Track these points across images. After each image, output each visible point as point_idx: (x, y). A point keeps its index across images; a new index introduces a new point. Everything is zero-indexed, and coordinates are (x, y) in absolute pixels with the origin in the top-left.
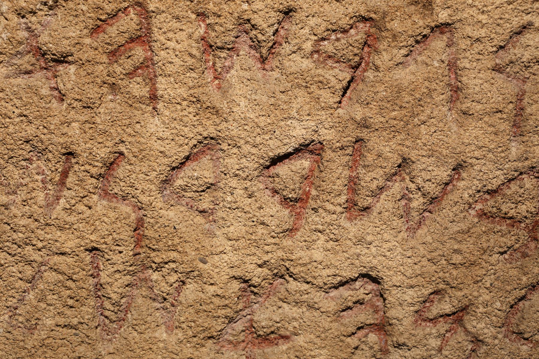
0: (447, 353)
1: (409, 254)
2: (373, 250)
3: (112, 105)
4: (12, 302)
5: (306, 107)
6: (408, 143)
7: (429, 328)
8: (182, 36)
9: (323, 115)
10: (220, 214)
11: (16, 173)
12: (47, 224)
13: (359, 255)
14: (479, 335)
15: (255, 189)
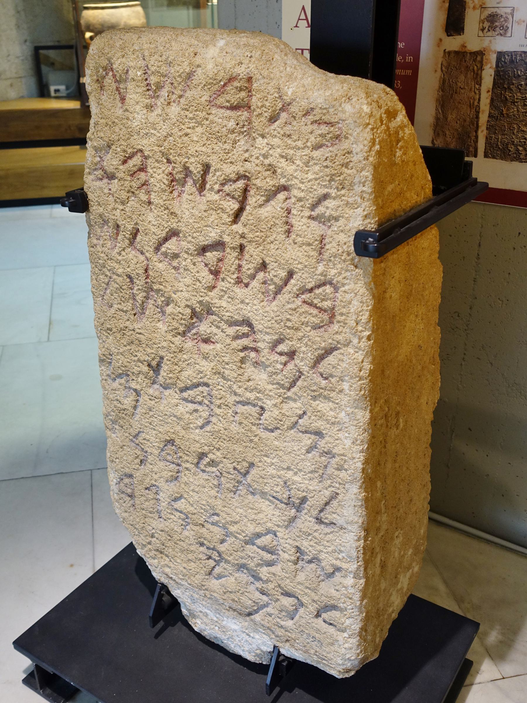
0: (285, 373)
1: (266, 315)
2: (249, 308)
3: (133, 203)
4: (102, 293)
5: (216, 221)
6: (265, 252)
7: (277, 357)
8: (160, 171)
9: (224, 228)
11: (99, 230)
12: (111, 259)
13: (242, 309)
14: (301, 369)
15: (196, 260)
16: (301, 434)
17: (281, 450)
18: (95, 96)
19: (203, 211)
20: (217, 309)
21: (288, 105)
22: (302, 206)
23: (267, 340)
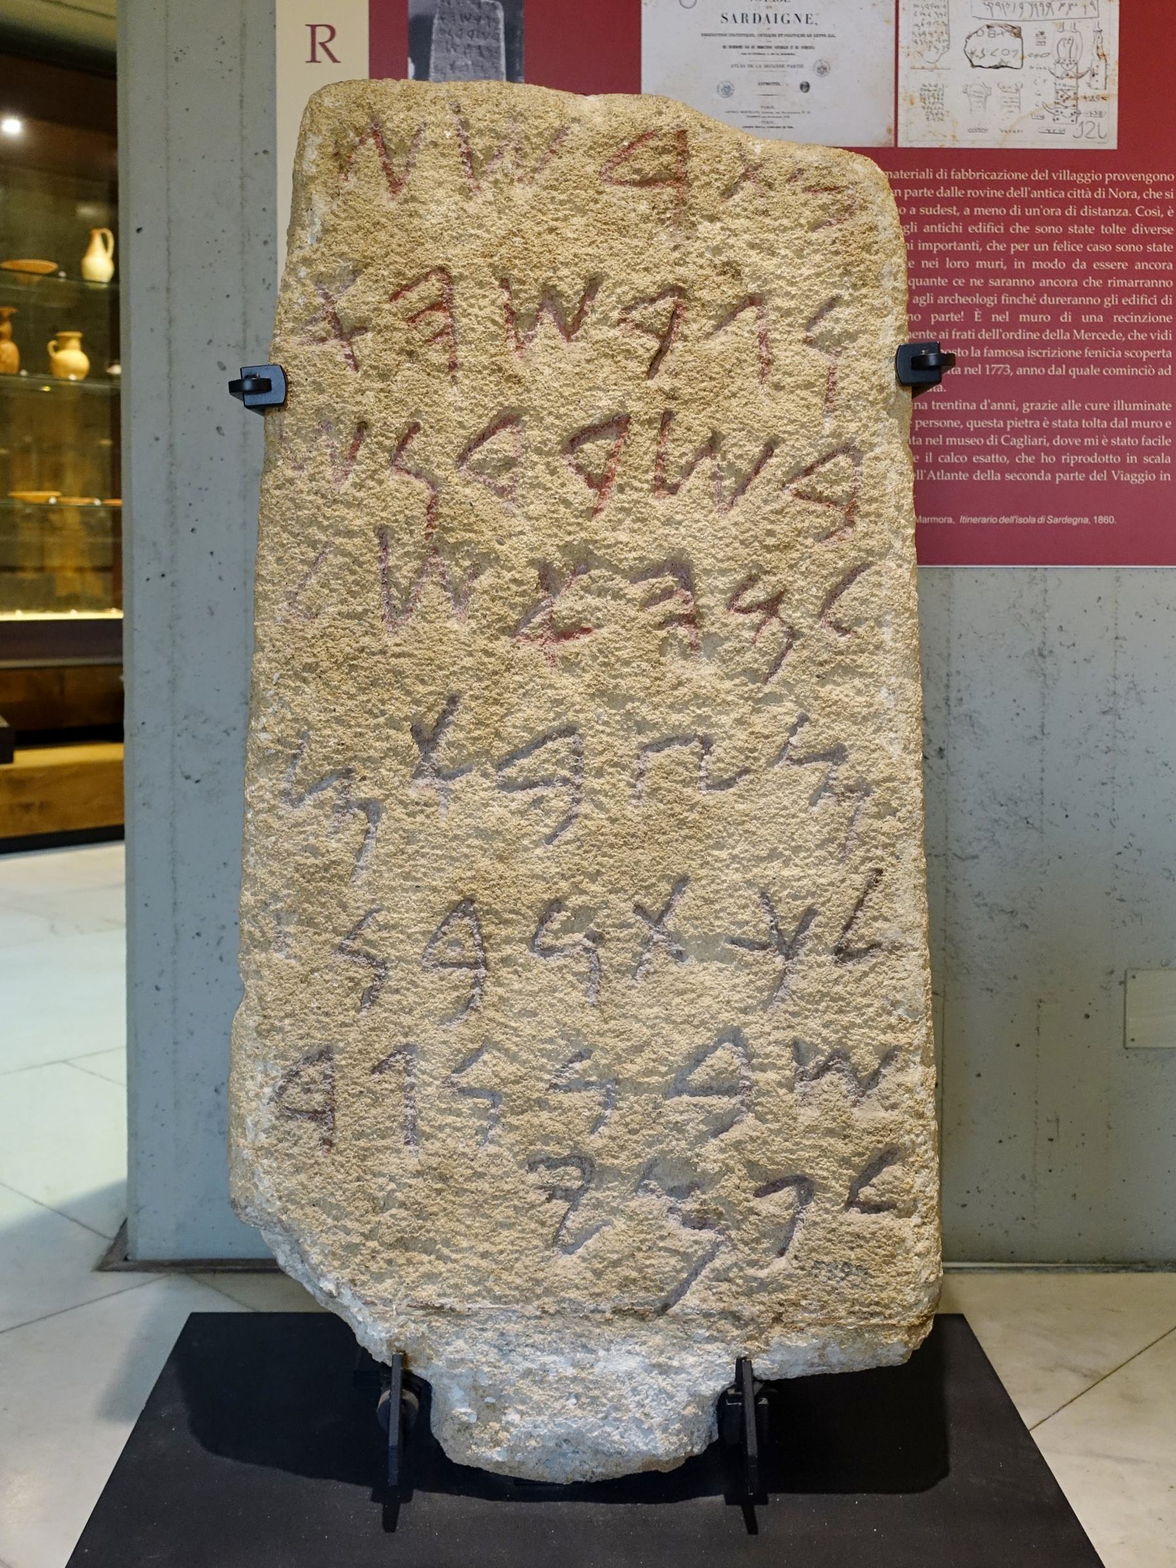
3: (408, 373)
10: (519, 491)
16: (796, 767)
17: (755, 818)
18: (325, 184)
19: (583, 362)
20: (609, 551)
21: (756, 169)
22: (789, 325)
23: (721, 587)
